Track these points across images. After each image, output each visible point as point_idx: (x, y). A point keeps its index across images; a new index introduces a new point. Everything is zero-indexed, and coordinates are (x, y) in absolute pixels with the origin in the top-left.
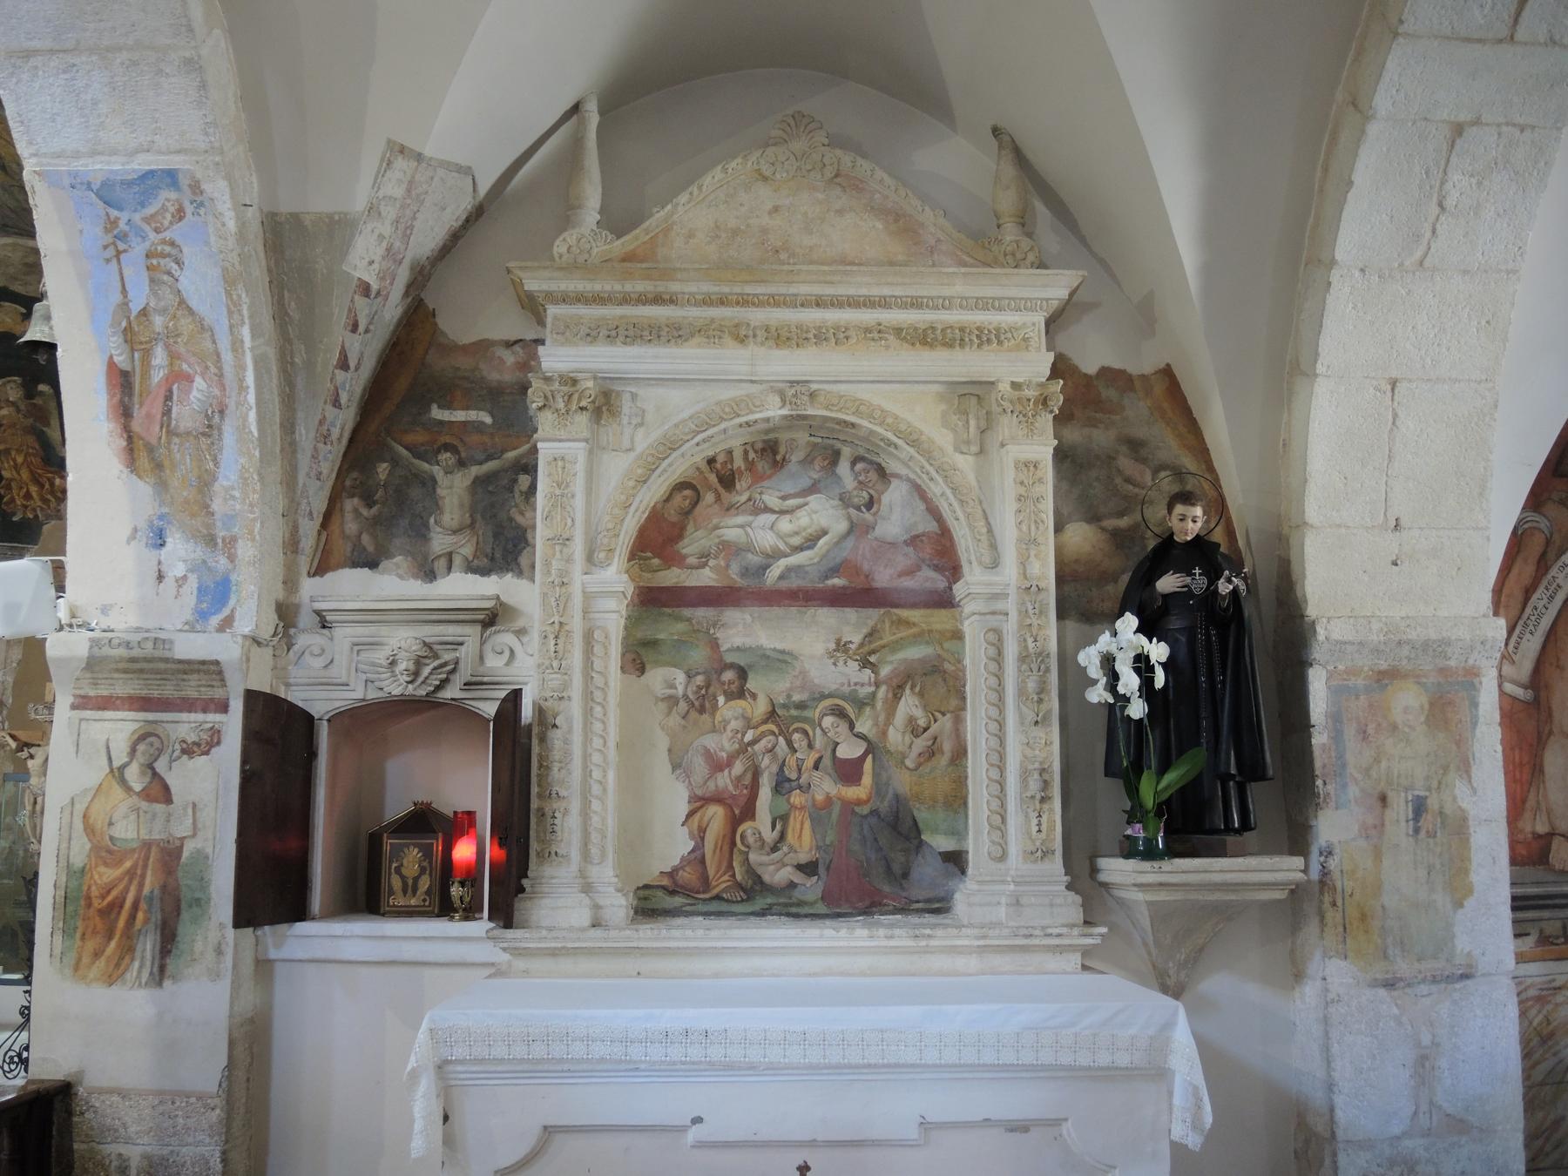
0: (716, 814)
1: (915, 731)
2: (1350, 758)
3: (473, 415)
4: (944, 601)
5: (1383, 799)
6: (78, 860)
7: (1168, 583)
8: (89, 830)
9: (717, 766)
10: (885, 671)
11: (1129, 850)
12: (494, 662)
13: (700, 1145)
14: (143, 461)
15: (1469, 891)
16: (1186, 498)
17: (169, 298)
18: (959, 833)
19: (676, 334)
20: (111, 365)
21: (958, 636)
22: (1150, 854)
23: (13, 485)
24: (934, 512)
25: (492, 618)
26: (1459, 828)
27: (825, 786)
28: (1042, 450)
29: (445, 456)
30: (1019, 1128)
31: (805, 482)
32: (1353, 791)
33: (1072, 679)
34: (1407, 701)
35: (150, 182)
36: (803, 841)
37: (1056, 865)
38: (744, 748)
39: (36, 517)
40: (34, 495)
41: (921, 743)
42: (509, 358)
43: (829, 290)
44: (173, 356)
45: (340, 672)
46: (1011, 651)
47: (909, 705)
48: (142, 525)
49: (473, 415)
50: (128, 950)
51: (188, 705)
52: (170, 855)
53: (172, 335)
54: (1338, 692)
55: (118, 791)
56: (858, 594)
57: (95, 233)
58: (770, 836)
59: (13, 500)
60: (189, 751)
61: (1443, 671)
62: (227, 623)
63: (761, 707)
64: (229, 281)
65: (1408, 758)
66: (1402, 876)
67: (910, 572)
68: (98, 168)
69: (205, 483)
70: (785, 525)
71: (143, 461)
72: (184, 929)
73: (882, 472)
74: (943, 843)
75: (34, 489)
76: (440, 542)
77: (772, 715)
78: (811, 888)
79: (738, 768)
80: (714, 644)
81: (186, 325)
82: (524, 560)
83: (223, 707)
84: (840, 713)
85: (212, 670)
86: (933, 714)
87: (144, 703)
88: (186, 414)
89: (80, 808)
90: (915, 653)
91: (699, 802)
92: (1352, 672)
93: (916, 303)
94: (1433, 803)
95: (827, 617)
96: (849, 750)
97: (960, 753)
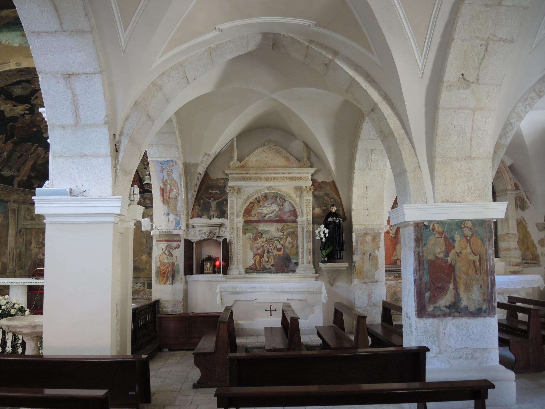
0: (258, 257)
1: (290, 243)
2: (359, 247)
3: (216, 191)
4: (295, 221)
5: (364, 254)
6: (158, 265)
7: (330, 219)
8: (160, 261)
9: (258, 249)
10: (285, 233)
12: (221, 233)
13: (256, 303)
14: (165, 202)
15: (378, 268)
16: (333, 205)
17: (170, 178)
18: (297, 260)
19: (250, 179)
20: (161, 188)
21: (297, 227)
24: (293, 207)
25: (221, 226)
26: (377, 258)
27: (275, 252)
28: (310, 197)
29: (212, 199)
30: (301, 300)
31: (272, 202)
32: (359, 252)
34: (369, 238)
35: (168, 161)
36: (272, 261)
37: (312, 264)
38: (262, 246)
41: (291, 245)
42: (222, 182)
43: (275, 172)
44: (171, 186)
45: (197, 235)
46: (305, 230)
47: (289, 239)
48: (166, 212)
49: (216, 191)
50: (167, 279)
51: (175, 241)
52: (173, 264)
53: (171, 183)
54: (357, 237)
55: (164, 255)
56: (280, 220)
57: (159, 168)
58: (266, 260)
60: (175, 248)
61: (375, 233)
62: (180, 228)
63: (265, 239)
64: (180, 175)
65: (368, 247)
66: (367, 266)
67: (289, 217)
68: (160, 159)
69: (176, 206)
70: (268, 209)
71: (165, 202)
72: (176, 276)
73: (284, 200)
74: (295, 261)
76: (212, 213)
77: (267, 241)
78: (273, 269)
79: (261, 249)
80: (257, 229)
81: (173, 181)
82: (226, 216)
83: (180, 241)
84: (278, 240)
85: (179, 236)
86: (293, 240)
87: (167, 241)
88: (173, 194)
89: (158, 258)
90: (290, 230)
91: (255, 255)
92: (360, 233)
93: (290, 173)
94: (372, 254)
95: (275, 224)
96: (279, 246)
97: (297, 247)
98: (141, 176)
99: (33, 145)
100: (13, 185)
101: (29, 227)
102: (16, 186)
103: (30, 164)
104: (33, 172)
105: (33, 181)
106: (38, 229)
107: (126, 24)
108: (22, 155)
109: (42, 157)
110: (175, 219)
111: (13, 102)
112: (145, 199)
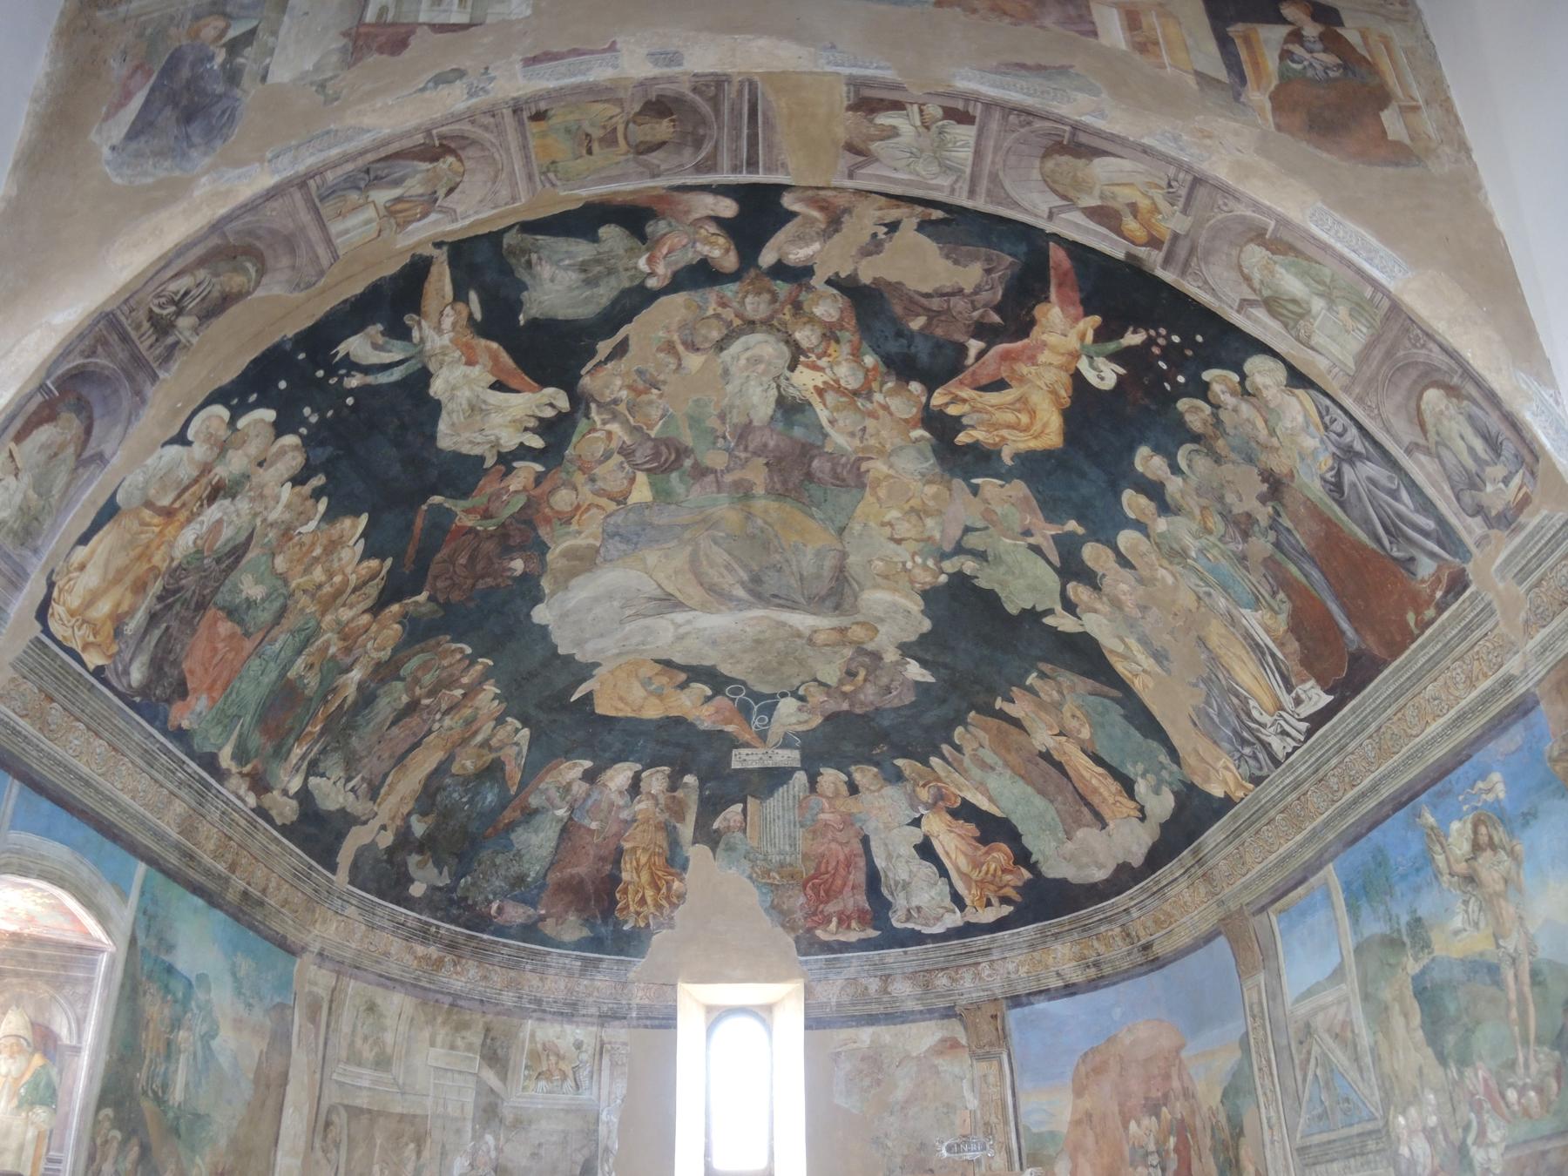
23: (631, 888)
39: (648, 925)
40: (649, 900)
59: (627, 907)
75: (649, 893)
98: (880, 863)
99: (472, 660)
100: (333, 868)
101: (362, 1101)
102: (341, 878)
103: (424, 764)
104: (424, 814)
105: (413, 859)
106: (402, 1117)
108: (413, 707)
109: (479, 738)
111: (505, 358)
112: (886, 978)
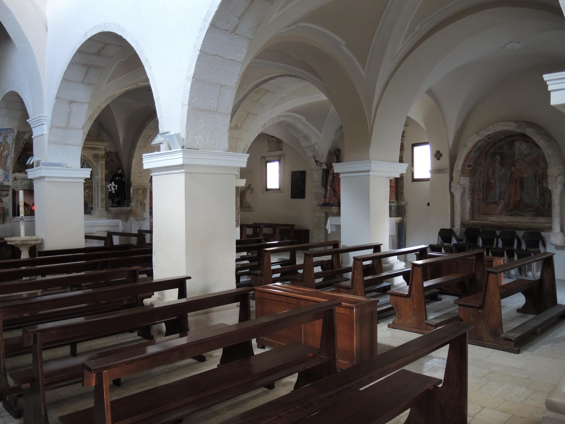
7: (117, 178)
11: (112, 206)
16: (119, 169)
22: (115, 207)
26: (145, 204)
28: (104, 163)
33: (107, 189)
34: (140, 191)
37: (104, 208)
51: (5, 191)
53: (4, 145)
54: (134, 190)
60: (5, 196)
62: (8, 181)
64: (13, 140)
69: (5, 163)
74: (90, 206)
81: (6, 144)
85: (8, 186)
107: (109, 81)
110: (5, 173)
